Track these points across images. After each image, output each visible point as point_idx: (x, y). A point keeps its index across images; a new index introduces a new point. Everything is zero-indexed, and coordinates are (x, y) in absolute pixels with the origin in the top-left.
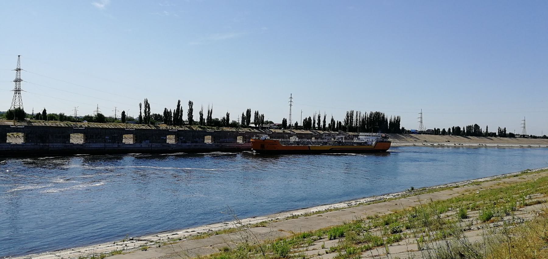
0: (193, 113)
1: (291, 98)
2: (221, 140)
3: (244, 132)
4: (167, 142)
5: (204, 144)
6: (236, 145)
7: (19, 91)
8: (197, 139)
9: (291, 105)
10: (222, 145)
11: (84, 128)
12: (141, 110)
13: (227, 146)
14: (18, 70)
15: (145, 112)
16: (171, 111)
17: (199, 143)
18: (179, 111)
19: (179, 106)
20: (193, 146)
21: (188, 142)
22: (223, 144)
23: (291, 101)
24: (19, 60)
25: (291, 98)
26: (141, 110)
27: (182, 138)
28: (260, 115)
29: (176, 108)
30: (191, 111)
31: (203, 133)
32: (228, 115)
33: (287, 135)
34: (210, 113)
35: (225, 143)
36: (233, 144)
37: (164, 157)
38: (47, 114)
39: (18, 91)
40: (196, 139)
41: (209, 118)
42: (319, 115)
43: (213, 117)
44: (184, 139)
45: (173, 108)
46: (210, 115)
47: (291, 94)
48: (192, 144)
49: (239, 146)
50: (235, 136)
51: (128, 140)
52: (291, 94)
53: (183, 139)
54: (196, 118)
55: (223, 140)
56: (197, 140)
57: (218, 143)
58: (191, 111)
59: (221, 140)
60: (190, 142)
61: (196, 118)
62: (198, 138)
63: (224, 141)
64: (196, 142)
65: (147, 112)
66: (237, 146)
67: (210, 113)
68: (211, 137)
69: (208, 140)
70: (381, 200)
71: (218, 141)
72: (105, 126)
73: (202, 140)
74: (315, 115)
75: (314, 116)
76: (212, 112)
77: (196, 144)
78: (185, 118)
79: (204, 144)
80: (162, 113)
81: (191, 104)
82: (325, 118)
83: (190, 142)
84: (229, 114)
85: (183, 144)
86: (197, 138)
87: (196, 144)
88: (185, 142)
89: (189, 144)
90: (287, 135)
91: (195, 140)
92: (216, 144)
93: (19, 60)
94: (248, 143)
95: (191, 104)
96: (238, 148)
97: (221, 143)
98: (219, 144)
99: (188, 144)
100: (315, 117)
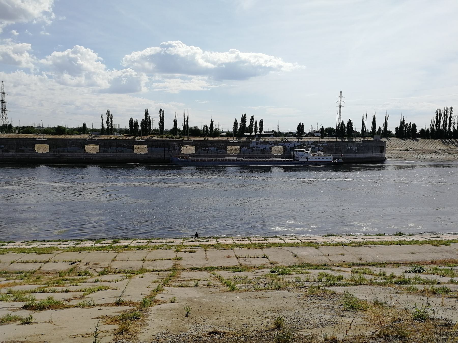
0: (376, 124)
1: (341, 97)
2: (58, 148)
3: (191, 140)
4: (182, 153)
5: (34, 153)
6: (83, 154)
7: (4, 110)
8: (24, 148)
9: (340, 106)
10: (61, 155)
11: (145, 140)
12: (102, 121)
13: (69, 155)
15: (108, 123)
16: (137, 121)
17: (27, 152)
18: (147, 121)
19: (146, 114)
20: (18, 155)
21: (10, 151)
22: (62, 153)
23: (341, 101)
25: (341, 97)
26: (102, 121)
27: (3, 146)
28: (256, 121)
29: (144, 118)
30: (162, 119)
31: (31, 141)
32: (212, 122)
33: (175, 143)
34: (186, 121)
35: (66, 152)
36: (78, 154)
37: (132, 167)
38: (164, 129)
40: (22, 148)
41: (186, 126)
42: (373, 117)
44: (6, 148)
45: (139, 118)
46: (186, 124)
47: (341, 92)
48: (17, 153)
49: (89, 156)
50: (131, 144)
51: (188, 150)
52: (341, 92)
53: (4, 148)
54: (168, 126)
55: (63, 149)
56: (23, 149)
57: (53, 152)
58: (162, 119)
59: (58, 148)
60: (14, 151)
61: (168, 126)
63: (64, 150)
64: (23, 151)
66: (85, 157)
67: (186, 121)
68: (145, 146)
69: (233, 150)
70: (202, 240)
71: (54, 150)
72: (62, 136)
73: (31, 149)
75: (363, 120)
76: (188, 119)
77: (23, 153)
78: (155, 126)
79: (34, 153)
81: (161, 112)
82: (374, 119)
83: (14, 151)
84: (213, 121)
85: (4, 153)
86: (23, 147)
87: (23, 153)
88: (8, 151)
89: (13, 153)
90: (175, 143)
91: (21, 149)
92: (52, 153)
93: (3, 84)
94: (103, 152)
95: (161, 112)
96: (86, 159)
97: (59, 152)
98: (56, 153)
99: (10, 153)
100: (365, 120)
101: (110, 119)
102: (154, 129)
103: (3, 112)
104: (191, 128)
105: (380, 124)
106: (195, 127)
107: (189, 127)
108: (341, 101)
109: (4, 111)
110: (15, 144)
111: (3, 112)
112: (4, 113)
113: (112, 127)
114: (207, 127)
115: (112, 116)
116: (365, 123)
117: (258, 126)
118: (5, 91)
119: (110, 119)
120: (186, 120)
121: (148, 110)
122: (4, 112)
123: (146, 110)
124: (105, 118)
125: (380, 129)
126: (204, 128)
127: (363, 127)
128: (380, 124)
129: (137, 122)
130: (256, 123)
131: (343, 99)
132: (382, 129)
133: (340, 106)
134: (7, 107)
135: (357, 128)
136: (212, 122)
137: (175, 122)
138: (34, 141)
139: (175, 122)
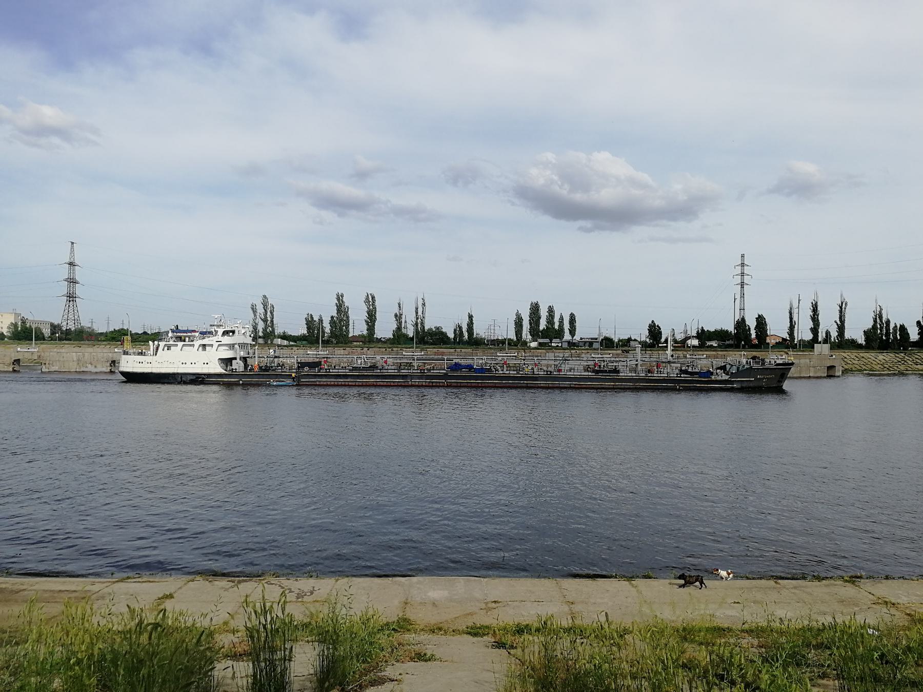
1: (743, 265)
9: (742, 285)
14: (71, 264)
23: (743, 274)
24: (72, 248)
25: (743, 265)
31: (105, 354)
32: (471, 317)
39: (71, 297)
40: (86, 367)
43: (429, 325)
45: (326, 313)
47: (743, 256)
52: (743, 256)
62: (92, 364)
65: (269, 322)
74: (795, 305)
78: (358, 327)
80: (731, 328)
81: (371, 301)
93: (72, 248)
95: (371, 301)
100: (795, 311)
101: (269, 313)
102: (356, 334)
103: (70, 301)
104: (431, 329)
105: (828, 323)
106: (438, 328)
107: (426, 328)
108: (743, 274)
109: (71, 299)
110: (75, 360)
111: (70, 301)
112: (71, 303)
113: (273, 330)
114: (460, 328)
115: (273, 308)
116: (795, 318)
117: (567, 326)
118: (77, 262)
119: (269, 313)
120: (420, 313)
121: (342, 296)
122: (73, 301)
123: (338, 295)
124: (260, 310)
125: (828, 333)
126: (455, 330)
127: (792, 328)
128: (828, 323)
129: (321, 320)
130: (562, 319)
131: (747, 270)
132: (834, 334)
133: (742, 285)
134: (79, 290)
135: (777, 329)
136: (471, 317)
137: (398, 317)
138: (110, 355)
139: (398, 317)
